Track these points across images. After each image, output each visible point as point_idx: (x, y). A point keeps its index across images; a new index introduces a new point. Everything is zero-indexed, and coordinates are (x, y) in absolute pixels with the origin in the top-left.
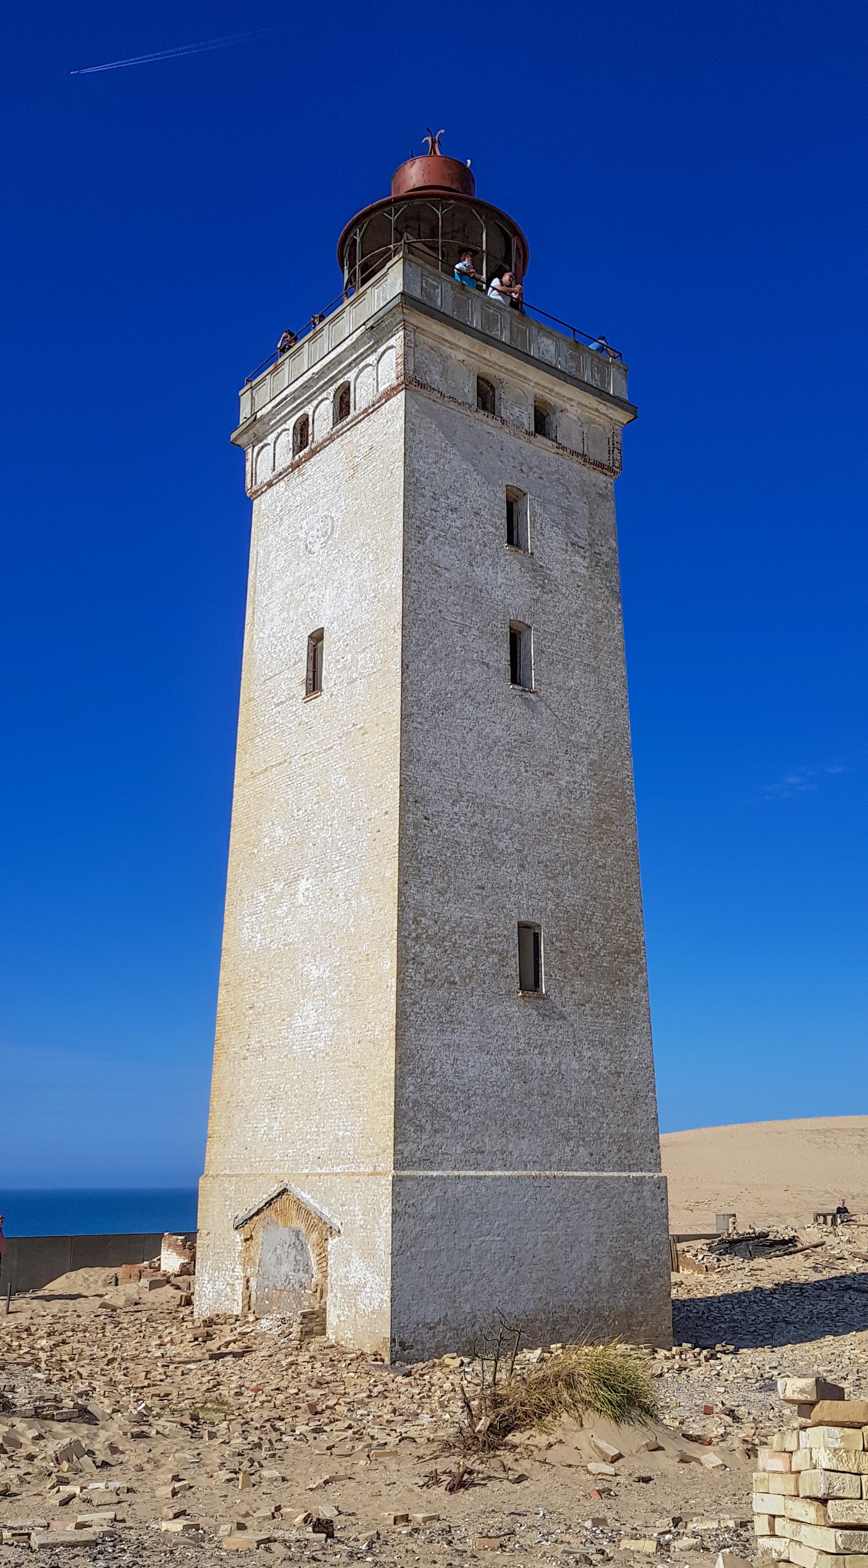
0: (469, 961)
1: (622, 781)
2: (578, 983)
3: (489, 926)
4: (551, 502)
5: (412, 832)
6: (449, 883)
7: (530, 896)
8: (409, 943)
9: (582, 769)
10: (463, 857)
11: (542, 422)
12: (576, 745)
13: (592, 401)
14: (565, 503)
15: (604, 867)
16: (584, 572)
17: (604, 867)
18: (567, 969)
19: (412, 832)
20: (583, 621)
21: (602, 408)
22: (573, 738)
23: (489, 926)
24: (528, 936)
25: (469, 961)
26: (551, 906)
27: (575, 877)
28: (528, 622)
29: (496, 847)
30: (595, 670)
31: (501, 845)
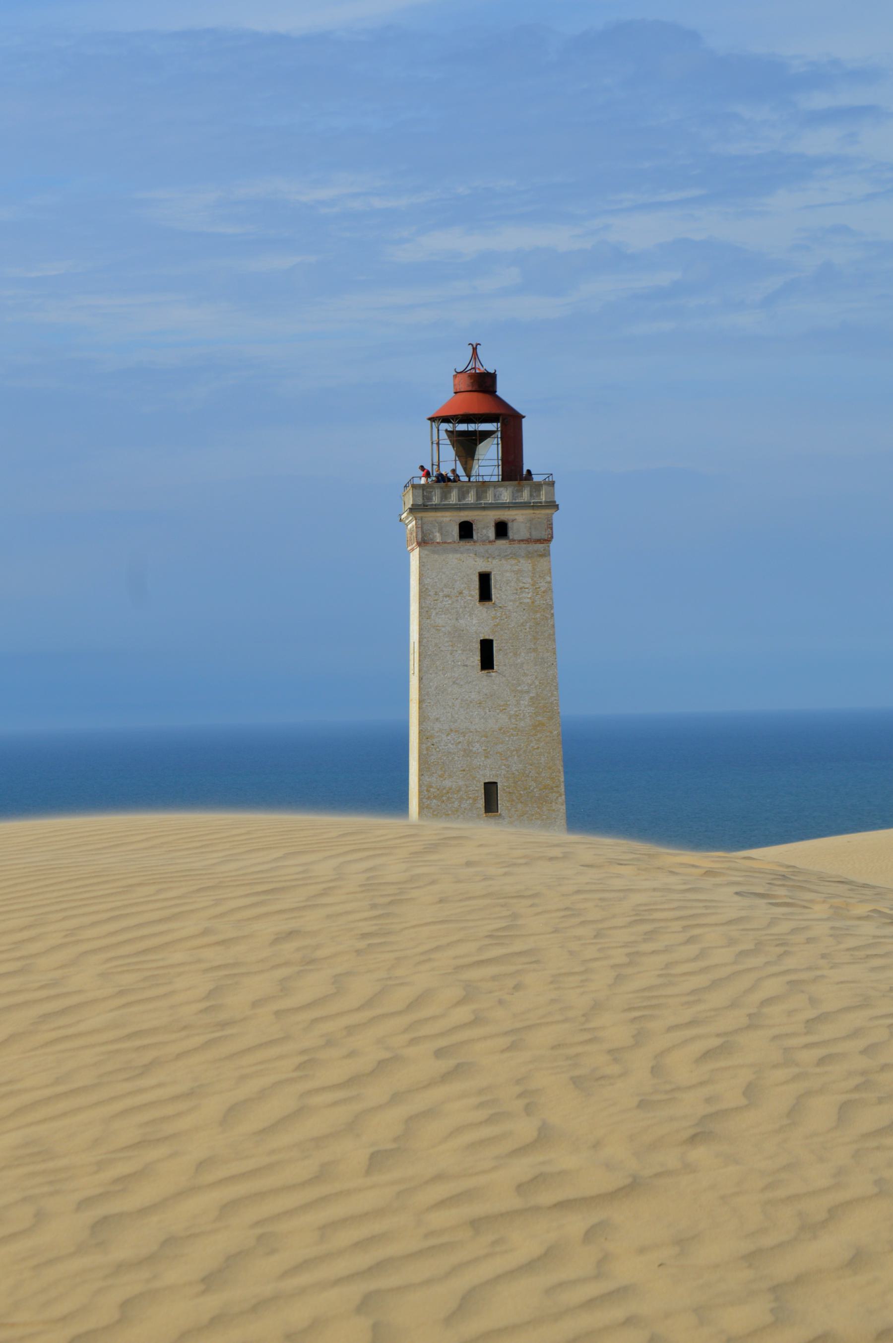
0: (456, 804)
1: (552, 703)
2: (520, 806)
3: (467, 787)
4: (507, 571)
5: (425, 752)
6: (445, 772)
7: (491, 769)
8: (424, 800)
9: (525, 702)
10: (453, 758)
11: (502, 529)
12: (521, 692)
13: (529, 512)
14: (516, 568)
15: (538, 748)
16: (528, 600)
17: (538, 748)
18: (513, 800)
19: (425, 752)
20: (527, 627)
21: (537, 512)
22: (519, 688)
23: (467, 787)
24: (490, 789)
25: (456, 804)
26: (504, 772)
27: (518, 757)
28: (491, 638)
29: (471, 751)
30: (535, 650)
31: (474, 749)
